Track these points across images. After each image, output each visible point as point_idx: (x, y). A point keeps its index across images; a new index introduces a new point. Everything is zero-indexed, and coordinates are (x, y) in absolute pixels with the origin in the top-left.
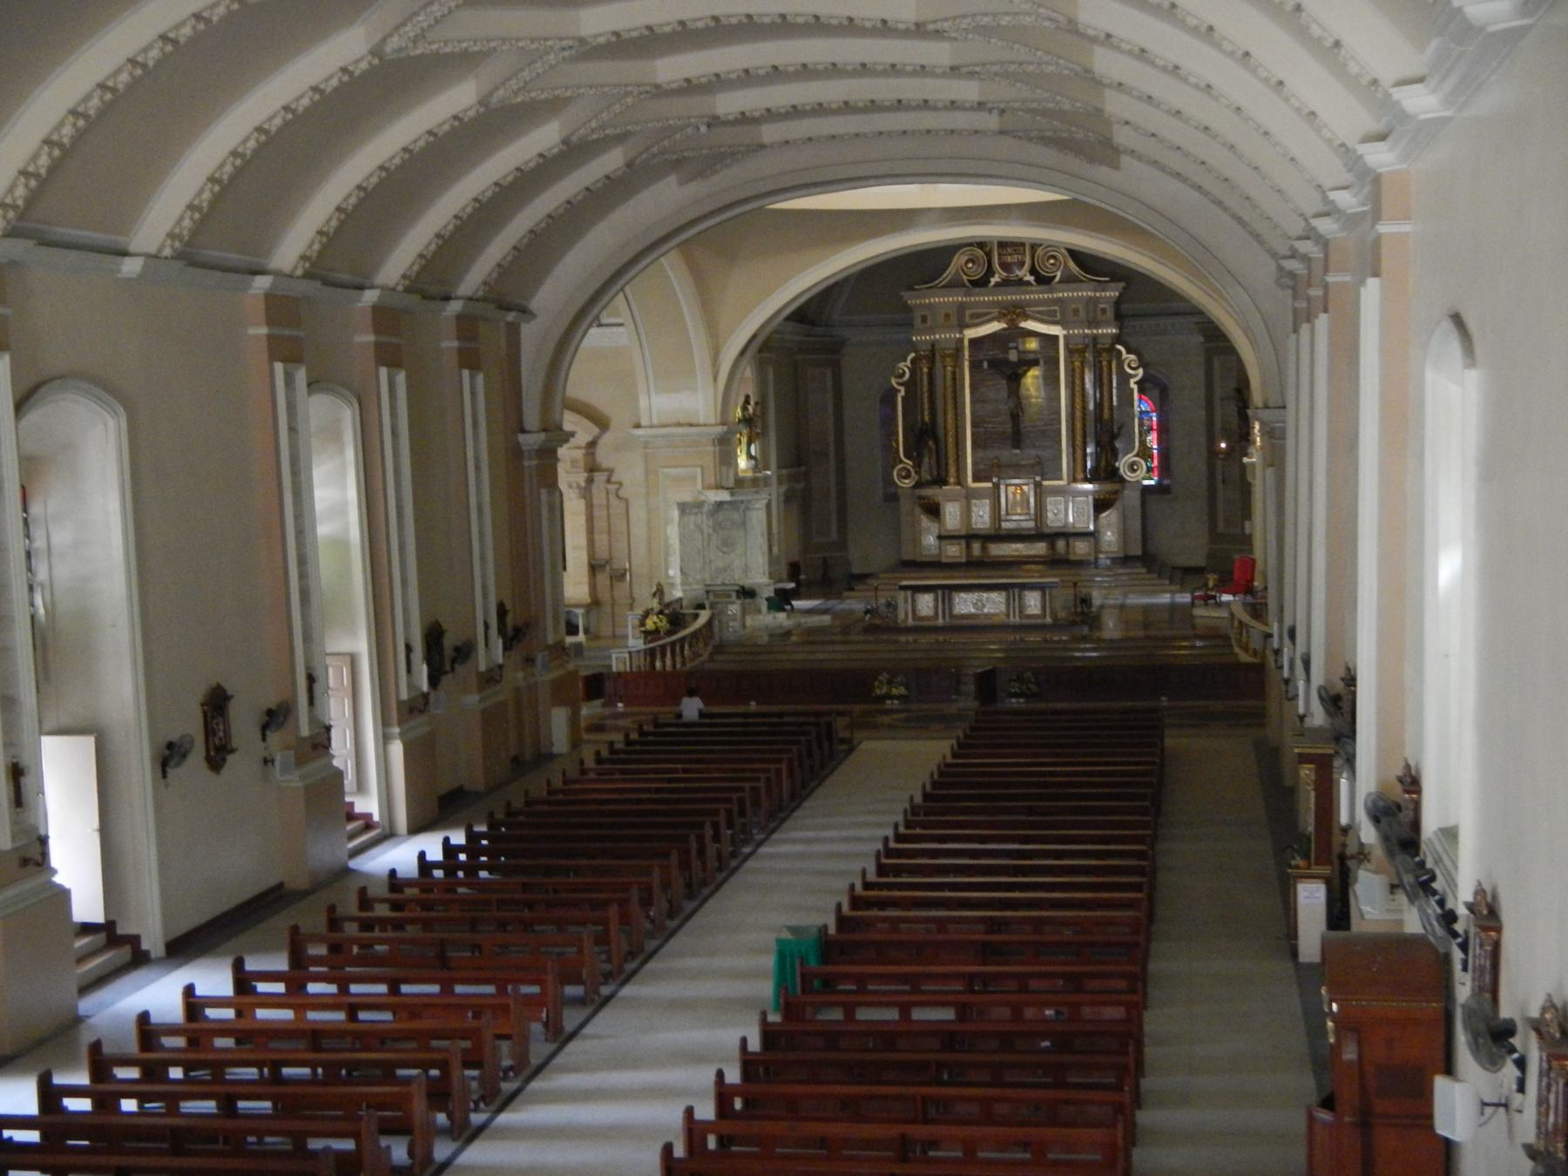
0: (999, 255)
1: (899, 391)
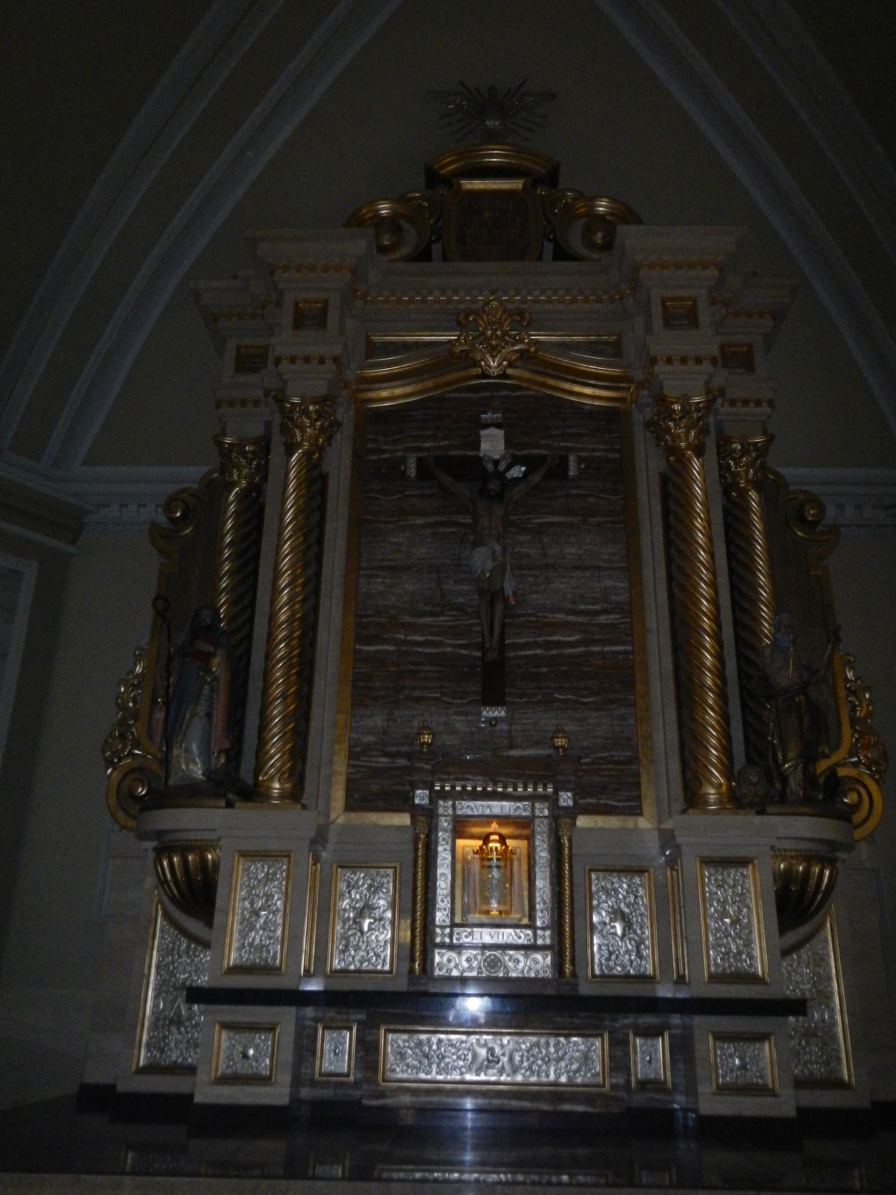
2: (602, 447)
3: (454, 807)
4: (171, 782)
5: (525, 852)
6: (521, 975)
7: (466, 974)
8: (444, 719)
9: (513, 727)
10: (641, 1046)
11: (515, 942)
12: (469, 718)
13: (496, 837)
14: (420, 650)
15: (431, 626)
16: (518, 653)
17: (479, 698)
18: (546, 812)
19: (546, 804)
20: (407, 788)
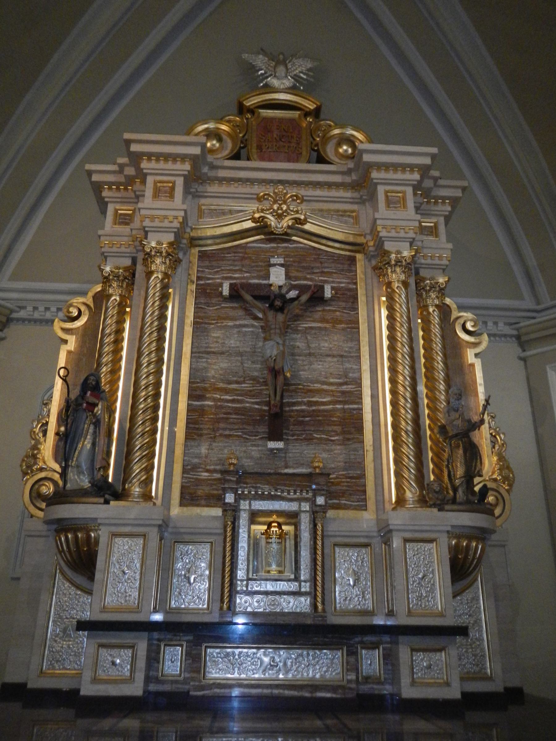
2: (344, 281)
3: (250, 505)
4: (68, 485)
5: (292, 533)
6: (291, 611)
7: (256, 610)
8: (244, 449)
9: (288, 455)
10: (366, 654)
11: (287, 590)
12: (260, 448)
13: (276, 524)
14: (230, 405)
15: (236, 390)
16: (291, 408)
17: (266, 436)
18: (308, 508)
19: (308, 504)
20: (220, 492)
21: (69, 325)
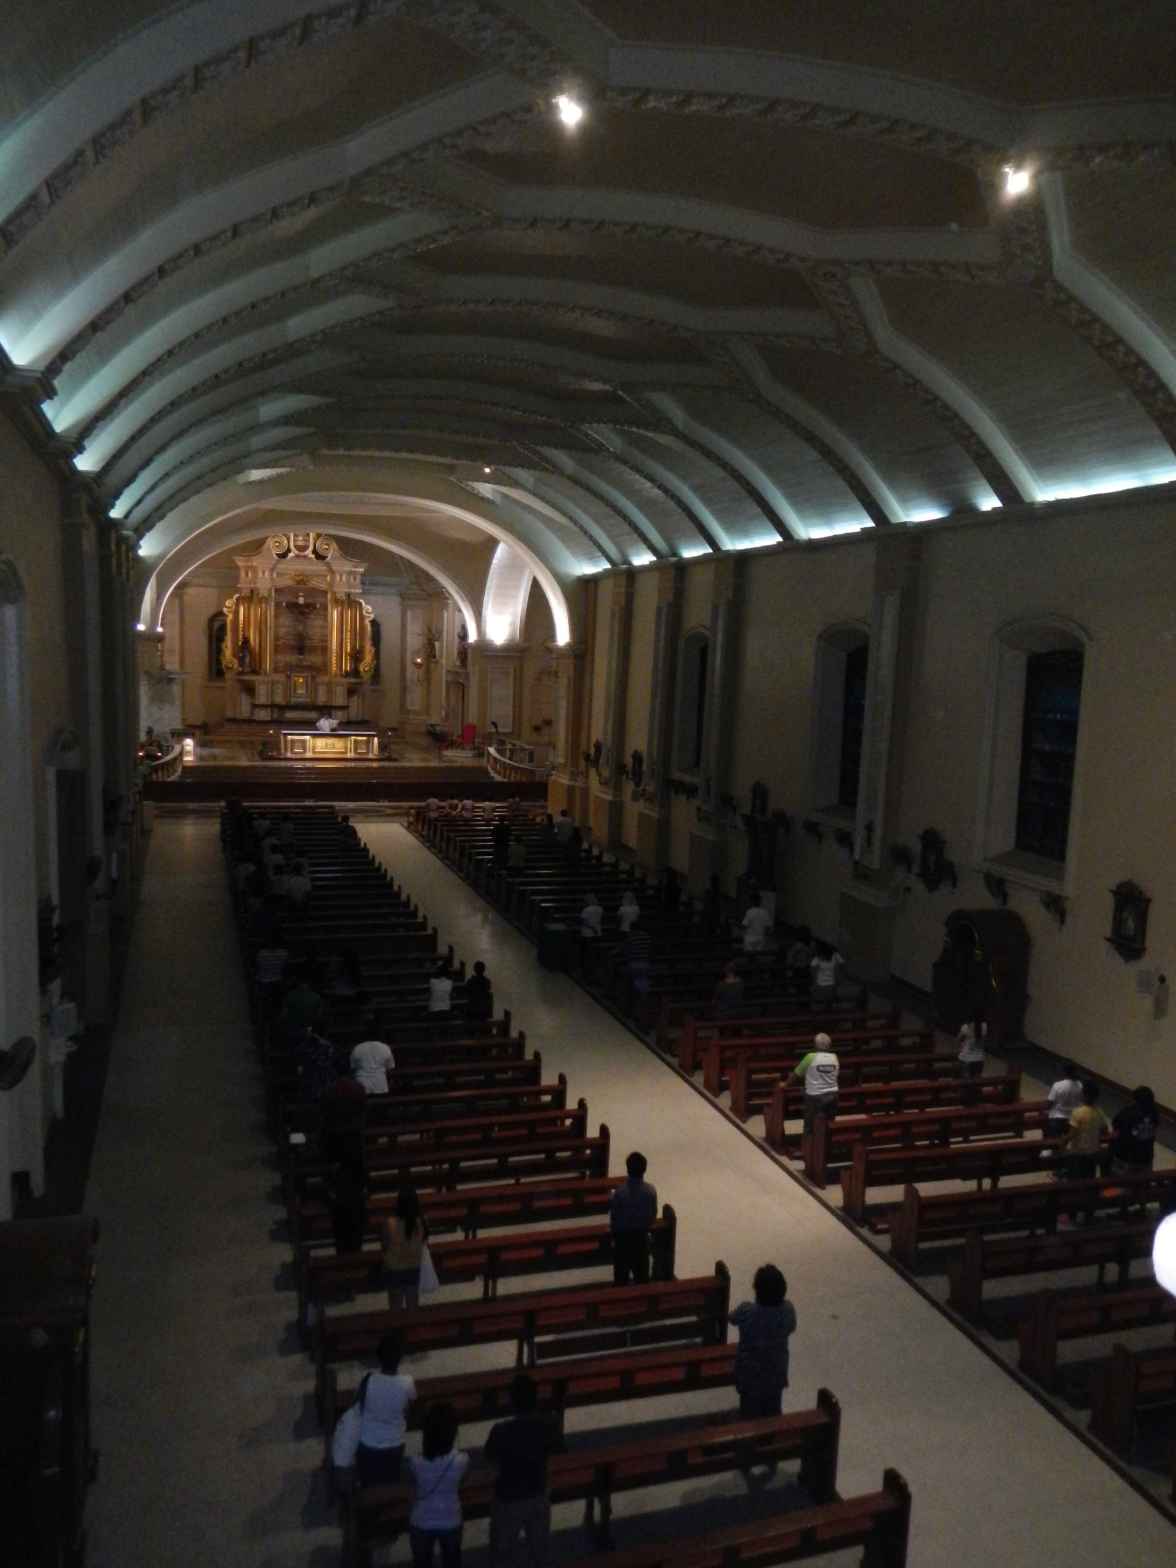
0: (294, 540)
1: (228, 616)
21: (229, 610)
